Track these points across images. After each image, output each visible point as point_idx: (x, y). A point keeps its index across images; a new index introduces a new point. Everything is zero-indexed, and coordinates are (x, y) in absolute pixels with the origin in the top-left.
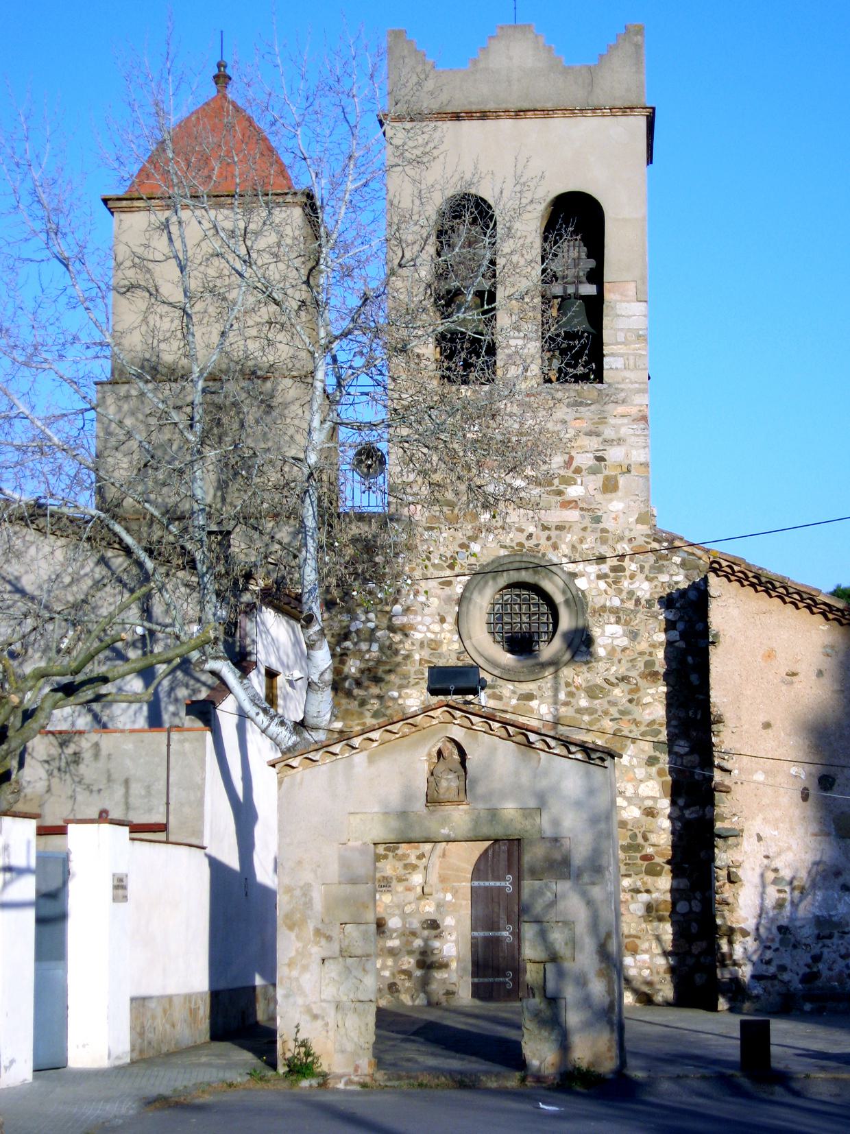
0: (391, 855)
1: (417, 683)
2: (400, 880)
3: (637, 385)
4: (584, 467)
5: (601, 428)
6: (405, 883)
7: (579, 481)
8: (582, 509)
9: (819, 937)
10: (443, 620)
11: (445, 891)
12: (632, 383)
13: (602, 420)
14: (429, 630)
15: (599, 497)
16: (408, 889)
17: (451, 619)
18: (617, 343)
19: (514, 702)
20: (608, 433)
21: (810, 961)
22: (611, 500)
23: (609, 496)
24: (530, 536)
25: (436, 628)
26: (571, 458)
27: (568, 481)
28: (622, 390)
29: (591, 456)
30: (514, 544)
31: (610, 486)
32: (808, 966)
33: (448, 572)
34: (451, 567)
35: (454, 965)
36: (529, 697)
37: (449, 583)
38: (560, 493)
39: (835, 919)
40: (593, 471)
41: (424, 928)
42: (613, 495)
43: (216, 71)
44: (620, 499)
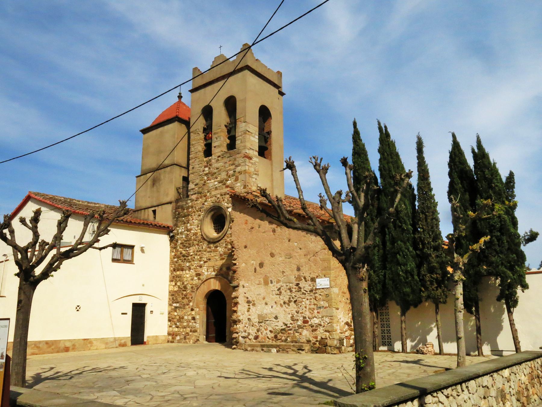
0: (185, 297)
1: (192, 246)
2: (187, 305)
3: (243, 147)
4: (231, 175)
5: (235, 162)
6: (188, 306)
7: (230, 179)
8: (230, 188)
9: (259, 323)
10: (198, 227)
11: (197, 307)
12: (242, 147)
13: (235, 160)
14: (195, 230)
15: (234, 183)
16: (189, 308)
17: (200, 226)
18: (239, 136)
19: (213, 248)
20: (236, 163)
21: (256, 331)
22: (237, 183)
23: (236, 182)
24: (218, 198)
25: (197, 229)
26: (228, 173)
27: (227, 180)
28: (240, 149)
29: (232, 171)
30: (214, 201)
31: (237, 179)
32: (256, 333)
33: (200, 212)
34: (200, 211)
35: (198, 331)
36: (216, 247)
37: (199, 215)
38: (225, 184)
39: (263, 315)
40: (233, 175)
41: (192, 320)
42: (237, 182)
43: (179, 95)
44: (239, 182)
